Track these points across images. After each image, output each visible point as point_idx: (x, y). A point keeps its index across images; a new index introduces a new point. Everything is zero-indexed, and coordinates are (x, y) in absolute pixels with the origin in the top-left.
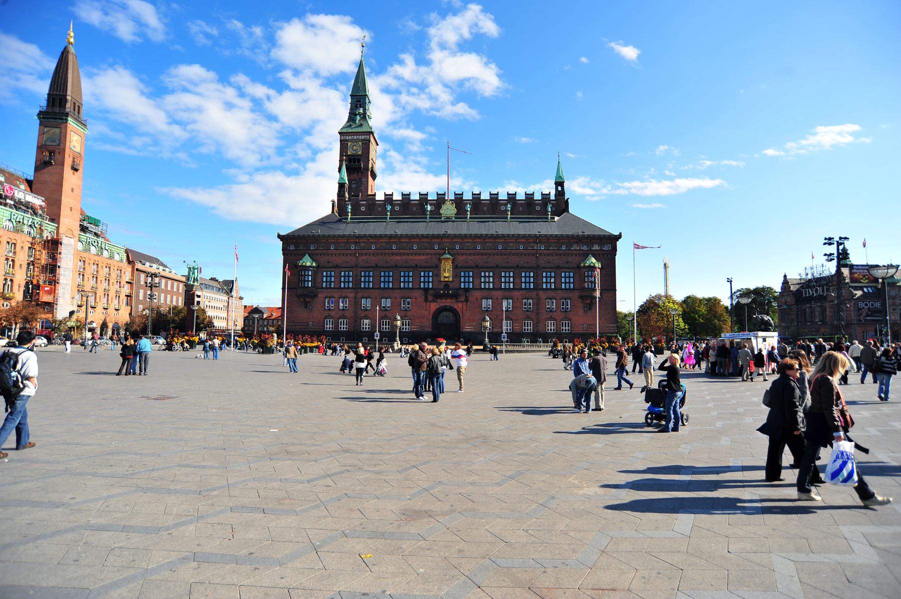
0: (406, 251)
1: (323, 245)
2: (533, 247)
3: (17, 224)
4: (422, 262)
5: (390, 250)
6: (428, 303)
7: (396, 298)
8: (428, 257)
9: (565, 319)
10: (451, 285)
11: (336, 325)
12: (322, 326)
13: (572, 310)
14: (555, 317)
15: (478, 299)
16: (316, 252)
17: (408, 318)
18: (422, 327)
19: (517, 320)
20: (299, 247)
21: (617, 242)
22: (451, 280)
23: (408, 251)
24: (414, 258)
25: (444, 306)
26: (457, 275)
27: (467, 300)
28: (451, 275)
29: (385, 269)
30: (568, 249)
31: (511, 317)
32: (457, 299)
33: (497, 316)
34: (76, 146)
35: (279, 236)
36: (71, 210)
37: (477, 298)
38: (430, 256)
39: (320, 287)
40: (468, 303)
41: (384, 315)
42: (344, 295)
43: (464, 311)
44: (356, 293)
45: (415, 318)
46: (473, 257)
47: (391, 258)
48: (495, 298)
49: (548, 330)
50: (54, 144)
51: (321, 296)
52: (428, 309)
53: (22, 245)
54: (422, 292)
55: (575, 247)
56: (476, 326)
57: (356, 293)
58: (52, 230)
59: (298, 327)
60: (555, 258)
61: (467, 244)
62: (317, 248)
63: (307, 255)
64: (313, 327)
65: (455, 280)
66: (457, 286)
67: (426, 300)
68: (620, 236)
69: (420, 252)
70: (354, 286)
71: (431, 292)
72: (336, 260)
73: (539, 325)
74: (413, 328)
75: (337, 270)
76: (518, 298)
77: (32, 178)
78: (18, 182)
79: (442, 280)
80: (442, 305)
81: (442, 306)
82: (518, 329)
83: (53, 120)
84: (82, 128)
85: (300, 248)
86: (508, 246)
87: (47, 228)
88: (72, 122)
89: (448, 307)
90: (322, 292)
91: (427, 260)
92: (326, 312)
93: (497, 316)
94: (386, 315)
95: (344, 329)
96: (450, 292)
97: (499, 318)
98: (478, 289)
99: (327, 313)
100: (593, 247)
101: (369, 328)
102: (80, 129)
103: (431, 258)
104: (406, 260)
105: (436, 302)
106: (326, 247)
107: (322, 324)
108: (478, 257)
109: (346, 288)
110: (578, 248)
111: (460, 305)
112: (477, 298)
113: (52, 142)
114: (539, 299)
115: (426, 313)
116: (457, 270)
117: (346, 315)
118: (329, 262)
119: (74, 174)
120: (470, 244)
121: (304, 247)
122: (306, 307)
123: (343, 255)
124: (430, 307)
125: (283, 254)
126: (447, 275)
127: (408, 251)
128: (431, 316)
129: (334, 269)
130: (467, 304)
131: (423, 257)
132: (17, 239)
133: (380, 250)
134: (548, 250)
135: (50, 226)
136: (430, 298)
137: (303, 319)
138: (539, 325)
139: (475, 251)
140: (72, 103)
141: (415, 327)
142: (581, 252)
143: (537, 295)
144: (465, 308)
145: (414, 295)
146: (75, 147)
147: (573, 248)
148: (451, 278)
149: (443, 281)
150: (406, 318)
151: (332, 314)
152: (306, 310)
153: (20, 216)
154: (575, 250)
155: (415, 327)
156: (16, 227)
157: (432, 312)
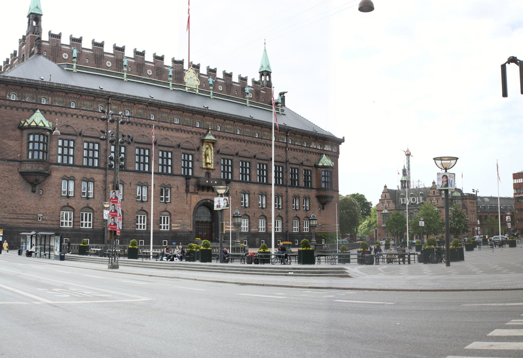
0: (165, 125)
1: (61, 99)
2: (283, 140)
4: (184, 140)
5: (148, 121)
6: (189, 195)
8: (190, 136)
9: (306, 219)
10: (213, 174)
11: (77, 220)
12: (57, 221)
13: (311, 209)
16: (49, 108)
18: (183, 225)
20: (25, 97)
21: (340, 146)
22: (212, 168)
23: (168, 125)
24: (174, 135)
25: (205, 200)
26: (218, 163)
28: (213, 162)
29: (141, 146)
30: (308, 146)
31: (266, 215)
33: (254, 214)
37: (236, 192)
38: (191, 135)
39: (54, 162)
41: (140, 208)
42: (88, 176)
44: (106, 175)
45: (175, 213)
46: (231, 143)
47: (148, 132)
48: (253, 192)
49: (62, 224)
51: (56, 175)
52: (189, 202)
54: (182, 179)
55: (313, 145)
57: (106, 175)
59: (21, 221)
60: (300, 154)
61: (228, 126)
62: (52, 103)
63: (38, 111)
64: (44, 222)
65: (216, 168)
67: (187, 191)
68: (343, 140)
69: (182, 128)
70: (102, 165)
71: (193, 181)
72: (77, 124)
74: (174, 227)
75: (79, 140)
79: (204, 166)
80: (204, 197)
81: (204, 200)
86: (264, 135)
89: (209, 201)
90: (57, 170)
91: (188, 140)
92: (64, 200)
93: (254, 214)
94: (142, 208)
95: (86, 226)
97: (256, 215)
98: (239, 181)
99: (64, 202)
100: (325, 147)
101: (90, 224)
103: (191, 137)
104: (166, 137)
105: (197, 193)
106: (64, 103)
107: (57, 218)
108: (237, 143)
109: (96, 168)
110: (315, 147)
112: (236, 192)
115: (187, 207)
116: (218, 156)
117: (91, 206)
118: (67, 126)
120: (230, 127)
121: (33, 98)
122: (34, 192)
123: (88, 118)
124: (191, 200)
126: (208, 161)
127: (165, 125)
128: (192, 211)
129: (74, 138)
131: (184, 135)
133: (136, 119)
134: (295, 145)
136: (192, 188)
137: (28, 208)
139: (235, 135)
141: (176, 225)
142: (317, 151)
143: (287, 192)
145: (175, 183)
147: (311, 146)
148: (213, 164)
149: (203, 168)
150: (165, 213)
151: (72, 203)
152: (34, 195)
154: (313, 148)
155: (176, 225)
157: (194, 204)
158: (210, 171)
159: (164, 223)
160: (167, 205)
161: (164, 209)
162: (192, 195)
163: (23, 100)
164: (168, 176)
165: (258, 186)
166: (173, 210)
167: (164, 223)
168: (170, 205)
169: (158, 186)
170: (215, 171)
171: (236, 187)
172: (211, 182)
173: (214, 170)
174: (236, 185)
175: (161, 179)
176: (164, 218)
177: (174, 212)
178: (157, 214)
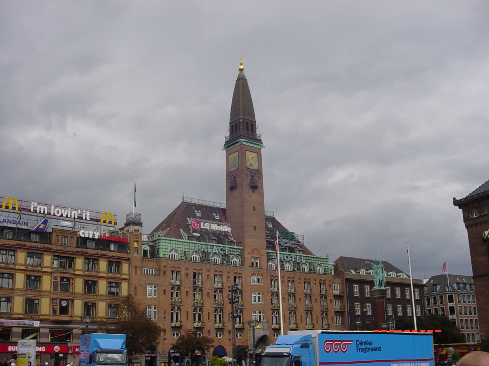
3: (202, 254)
20: (484, 211)
34: (253, 164)
35: (456, 203)
36: (255, 229)
50: (235, 168)
53: (207, 273)
58: (238, 253)
77: (223, 206)
78: (214, 214)
83: (233, 146)
84: (256, 144)
85: (486, 213)
87: (233, 253)
88: (246, 142)
102: (255, 146)
113: (234, 167)
119: (253, 192)
125: (467, 227)
132: (202, 268)
135: (235, 250)
140: (245, 123)
146: (251, 165)
153: (204, 246)
156: (202, 257)
163: (483, 214)
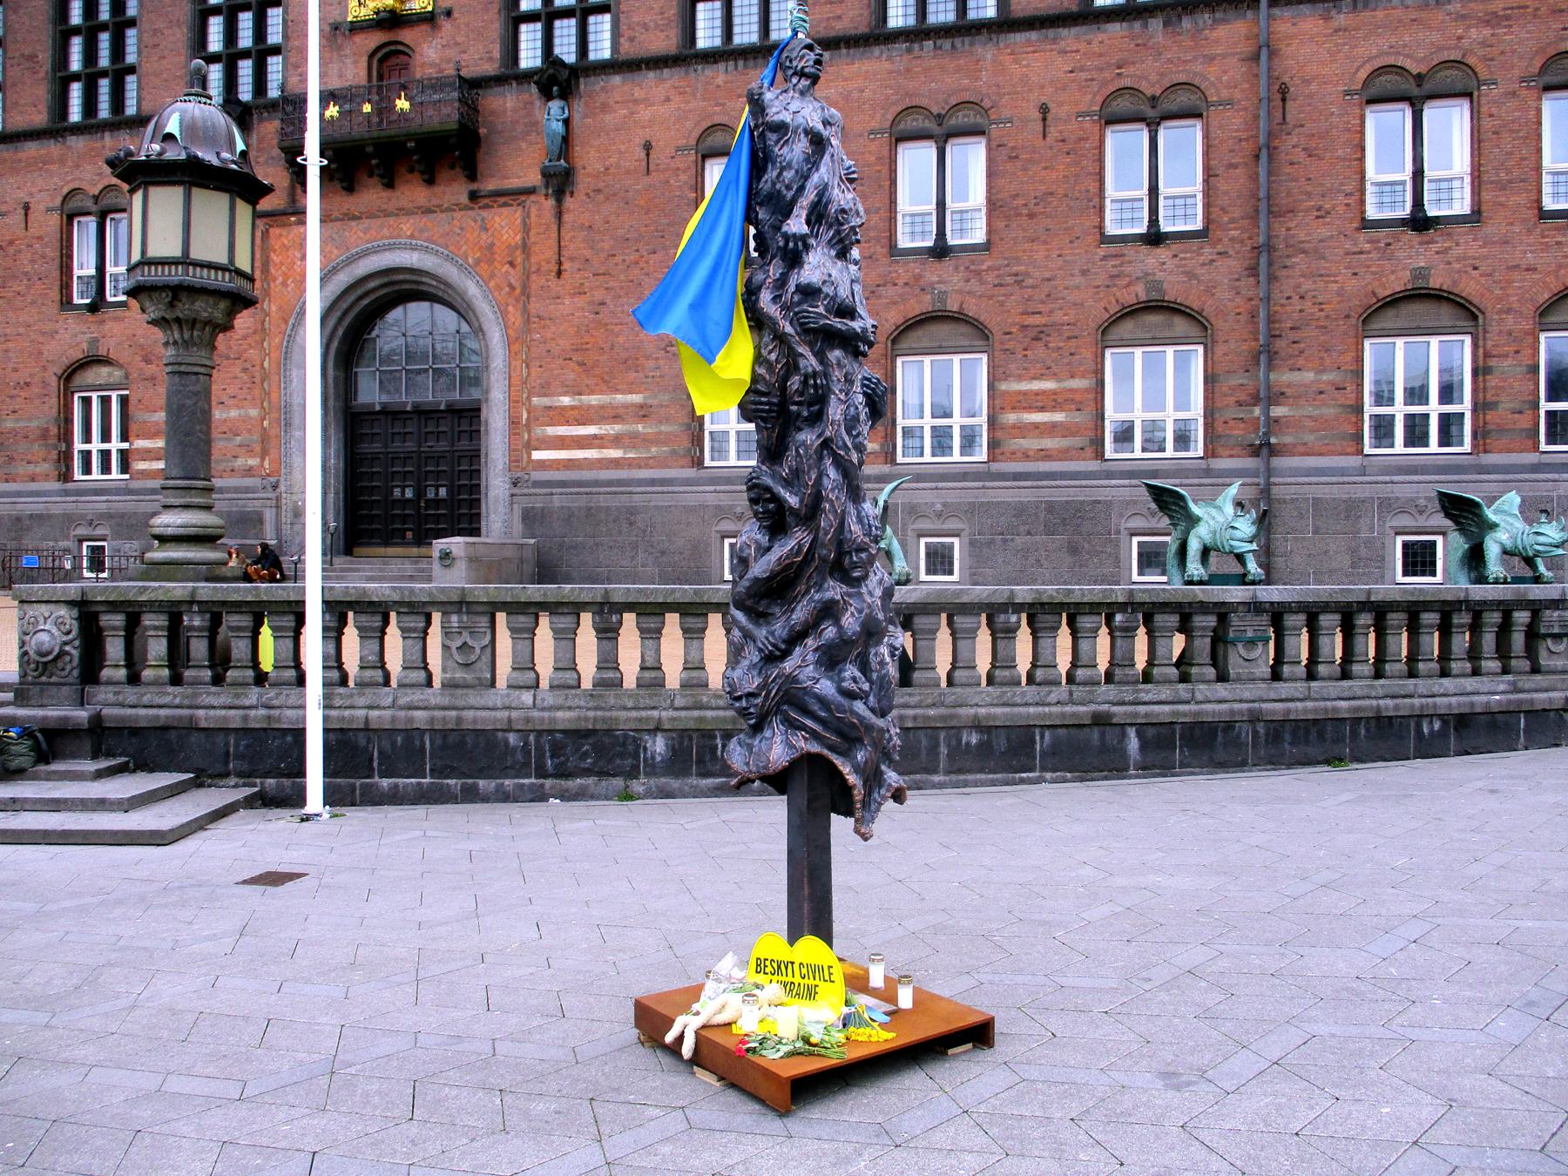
7: (27, 208)
14: (1469, 288)
15: (660, 156)
17: (118, 374)
19: (1039, 335)
27: (560, 181)
31: (971, 310)
32: (472, 176)
37: (648, 147)
40: (569, 202)
43: (536, 282)
56: (643, 412)
66: (481, 59)
73: (1283, 377)
76: (1044, 110)
82: (1051, 429)
96: (402, 104)
111: (504, 223)
112: (648, 147)
114: (1284, 92)
130: (559, 215)
138: (1283, 377)
144: (544, 252)
158: (407, 36)
159: (106, 437)
160: (103, 322)
161: (85, 346)
162: (274, 232)
164: (107, 135)
165: (887, 65)
166: (142, 347)
167: (106, 437)
168: (116, 319)
169: (49, 210)
170: (447, 26)
171: (645, 114)
172: (367, 108)
173: (442, 20)
174: (638, 93)
175: (62, 161)
176: (106, 401)
177: (148, 361)
178: (45, 384)
